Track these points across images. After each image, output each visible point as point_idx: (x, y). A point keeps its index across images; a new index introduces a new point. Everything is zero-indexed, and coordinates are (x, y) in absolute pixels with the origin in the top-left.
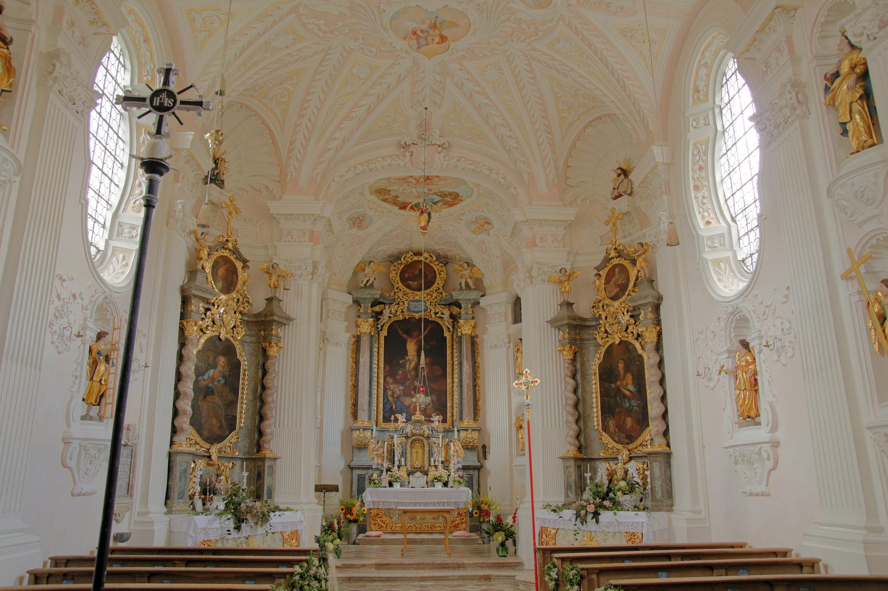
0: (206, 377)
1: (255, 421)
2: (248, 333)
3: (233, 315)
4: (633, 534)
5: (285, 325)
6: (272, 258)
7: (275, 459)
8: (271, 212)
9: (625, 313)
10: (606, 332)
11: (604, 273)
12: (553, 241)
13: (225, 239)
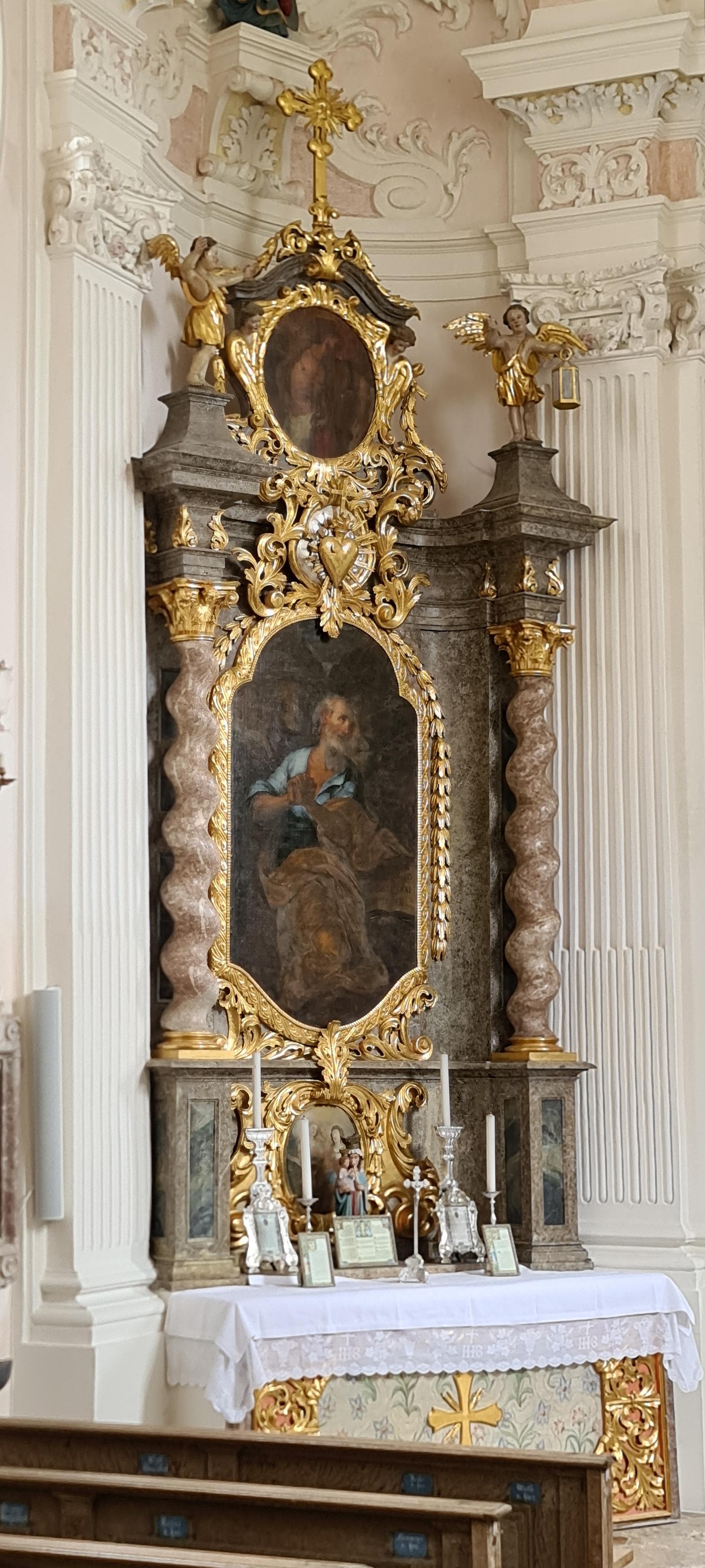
0: (279, 780)
1: (487, 930)
2: (437, 592)
3: (368, 535)
5: (578, 548)
6: (507, 284)
7: (571, 1074)
8: (487, 95)
13: (304, 245)
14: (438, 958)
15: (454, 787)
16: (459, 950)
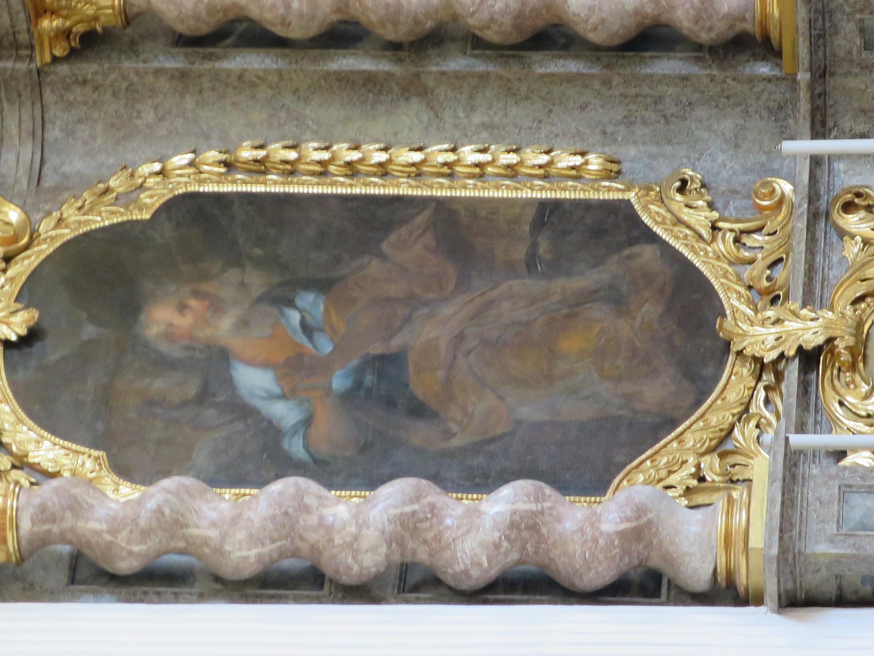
1: (569, 79)
14: (615, 167)
15: (316, 136)
16: (604, 133)
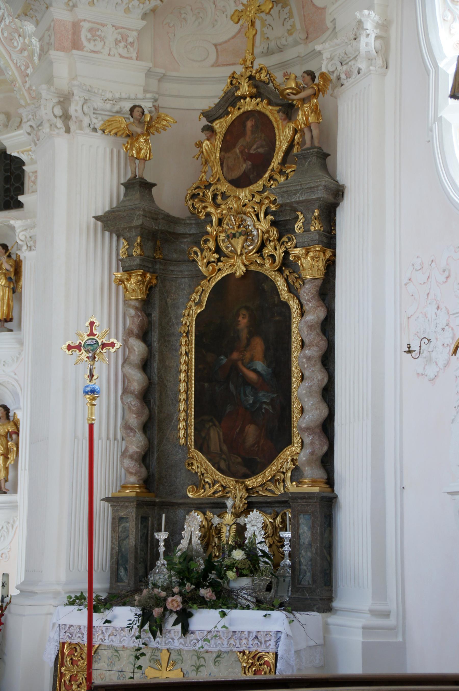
4: (257, 657)
9: (262, 216)
10: (218, 250)
11: (221, 127)
12: (117, 42)
